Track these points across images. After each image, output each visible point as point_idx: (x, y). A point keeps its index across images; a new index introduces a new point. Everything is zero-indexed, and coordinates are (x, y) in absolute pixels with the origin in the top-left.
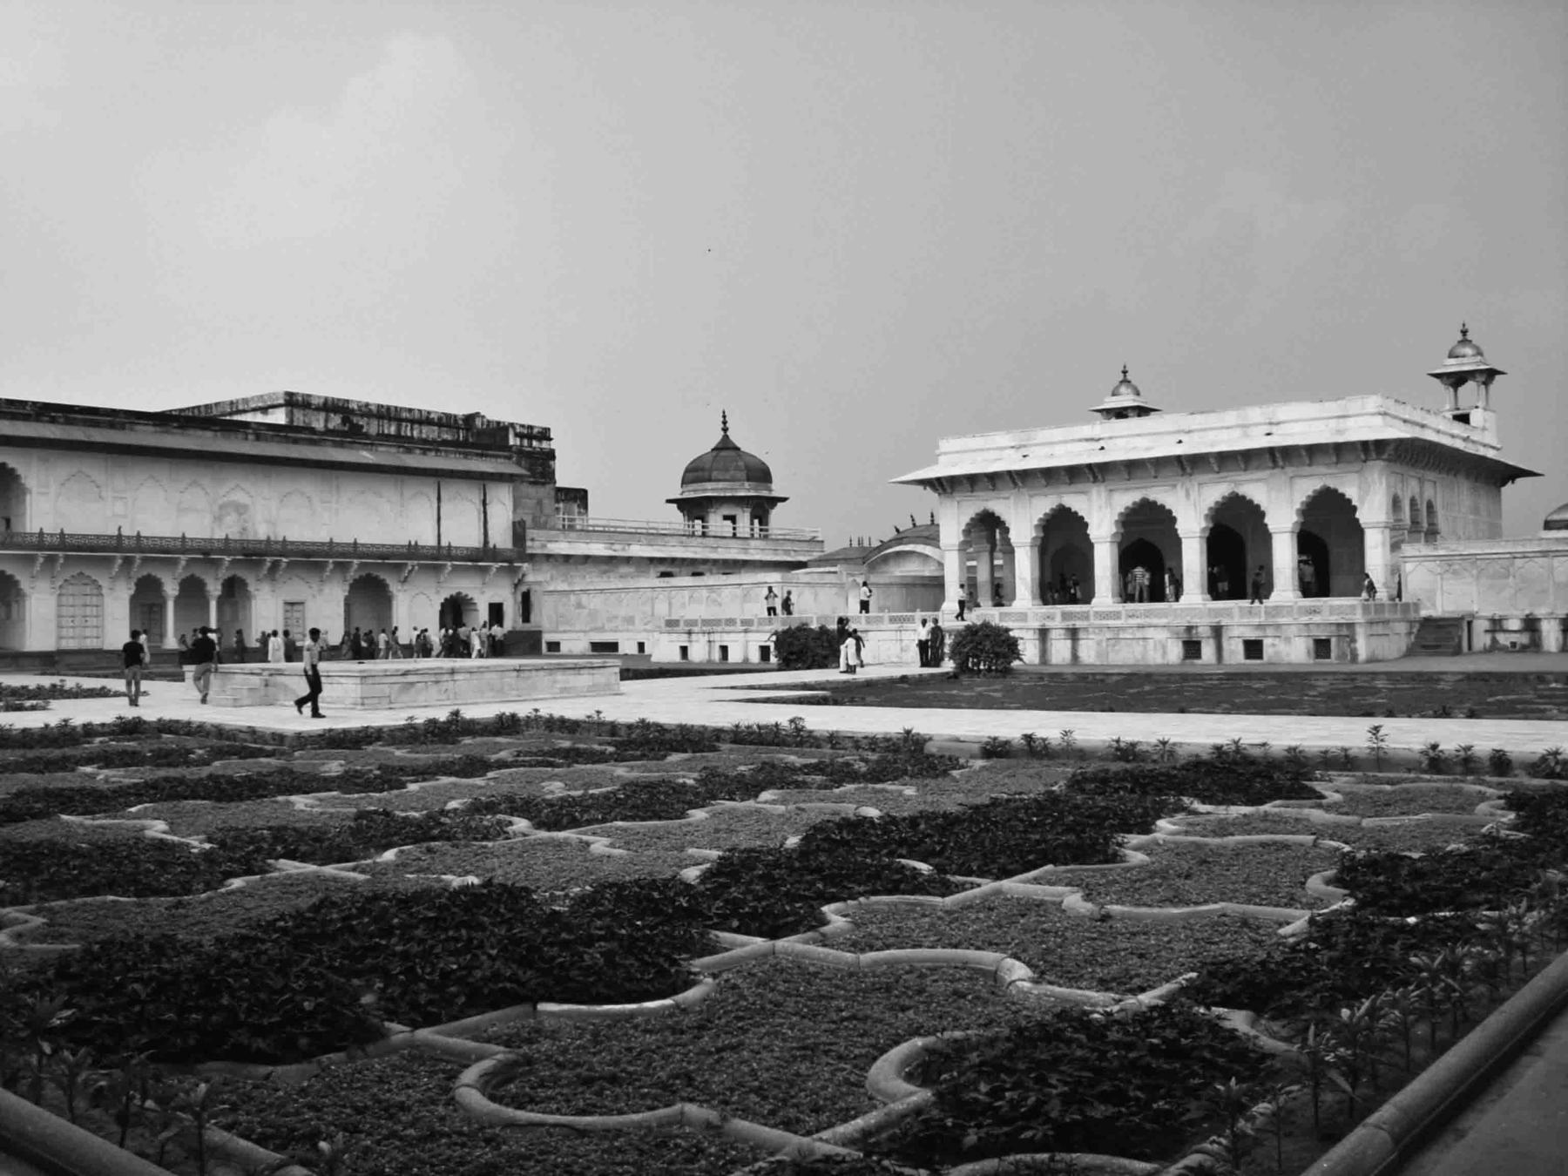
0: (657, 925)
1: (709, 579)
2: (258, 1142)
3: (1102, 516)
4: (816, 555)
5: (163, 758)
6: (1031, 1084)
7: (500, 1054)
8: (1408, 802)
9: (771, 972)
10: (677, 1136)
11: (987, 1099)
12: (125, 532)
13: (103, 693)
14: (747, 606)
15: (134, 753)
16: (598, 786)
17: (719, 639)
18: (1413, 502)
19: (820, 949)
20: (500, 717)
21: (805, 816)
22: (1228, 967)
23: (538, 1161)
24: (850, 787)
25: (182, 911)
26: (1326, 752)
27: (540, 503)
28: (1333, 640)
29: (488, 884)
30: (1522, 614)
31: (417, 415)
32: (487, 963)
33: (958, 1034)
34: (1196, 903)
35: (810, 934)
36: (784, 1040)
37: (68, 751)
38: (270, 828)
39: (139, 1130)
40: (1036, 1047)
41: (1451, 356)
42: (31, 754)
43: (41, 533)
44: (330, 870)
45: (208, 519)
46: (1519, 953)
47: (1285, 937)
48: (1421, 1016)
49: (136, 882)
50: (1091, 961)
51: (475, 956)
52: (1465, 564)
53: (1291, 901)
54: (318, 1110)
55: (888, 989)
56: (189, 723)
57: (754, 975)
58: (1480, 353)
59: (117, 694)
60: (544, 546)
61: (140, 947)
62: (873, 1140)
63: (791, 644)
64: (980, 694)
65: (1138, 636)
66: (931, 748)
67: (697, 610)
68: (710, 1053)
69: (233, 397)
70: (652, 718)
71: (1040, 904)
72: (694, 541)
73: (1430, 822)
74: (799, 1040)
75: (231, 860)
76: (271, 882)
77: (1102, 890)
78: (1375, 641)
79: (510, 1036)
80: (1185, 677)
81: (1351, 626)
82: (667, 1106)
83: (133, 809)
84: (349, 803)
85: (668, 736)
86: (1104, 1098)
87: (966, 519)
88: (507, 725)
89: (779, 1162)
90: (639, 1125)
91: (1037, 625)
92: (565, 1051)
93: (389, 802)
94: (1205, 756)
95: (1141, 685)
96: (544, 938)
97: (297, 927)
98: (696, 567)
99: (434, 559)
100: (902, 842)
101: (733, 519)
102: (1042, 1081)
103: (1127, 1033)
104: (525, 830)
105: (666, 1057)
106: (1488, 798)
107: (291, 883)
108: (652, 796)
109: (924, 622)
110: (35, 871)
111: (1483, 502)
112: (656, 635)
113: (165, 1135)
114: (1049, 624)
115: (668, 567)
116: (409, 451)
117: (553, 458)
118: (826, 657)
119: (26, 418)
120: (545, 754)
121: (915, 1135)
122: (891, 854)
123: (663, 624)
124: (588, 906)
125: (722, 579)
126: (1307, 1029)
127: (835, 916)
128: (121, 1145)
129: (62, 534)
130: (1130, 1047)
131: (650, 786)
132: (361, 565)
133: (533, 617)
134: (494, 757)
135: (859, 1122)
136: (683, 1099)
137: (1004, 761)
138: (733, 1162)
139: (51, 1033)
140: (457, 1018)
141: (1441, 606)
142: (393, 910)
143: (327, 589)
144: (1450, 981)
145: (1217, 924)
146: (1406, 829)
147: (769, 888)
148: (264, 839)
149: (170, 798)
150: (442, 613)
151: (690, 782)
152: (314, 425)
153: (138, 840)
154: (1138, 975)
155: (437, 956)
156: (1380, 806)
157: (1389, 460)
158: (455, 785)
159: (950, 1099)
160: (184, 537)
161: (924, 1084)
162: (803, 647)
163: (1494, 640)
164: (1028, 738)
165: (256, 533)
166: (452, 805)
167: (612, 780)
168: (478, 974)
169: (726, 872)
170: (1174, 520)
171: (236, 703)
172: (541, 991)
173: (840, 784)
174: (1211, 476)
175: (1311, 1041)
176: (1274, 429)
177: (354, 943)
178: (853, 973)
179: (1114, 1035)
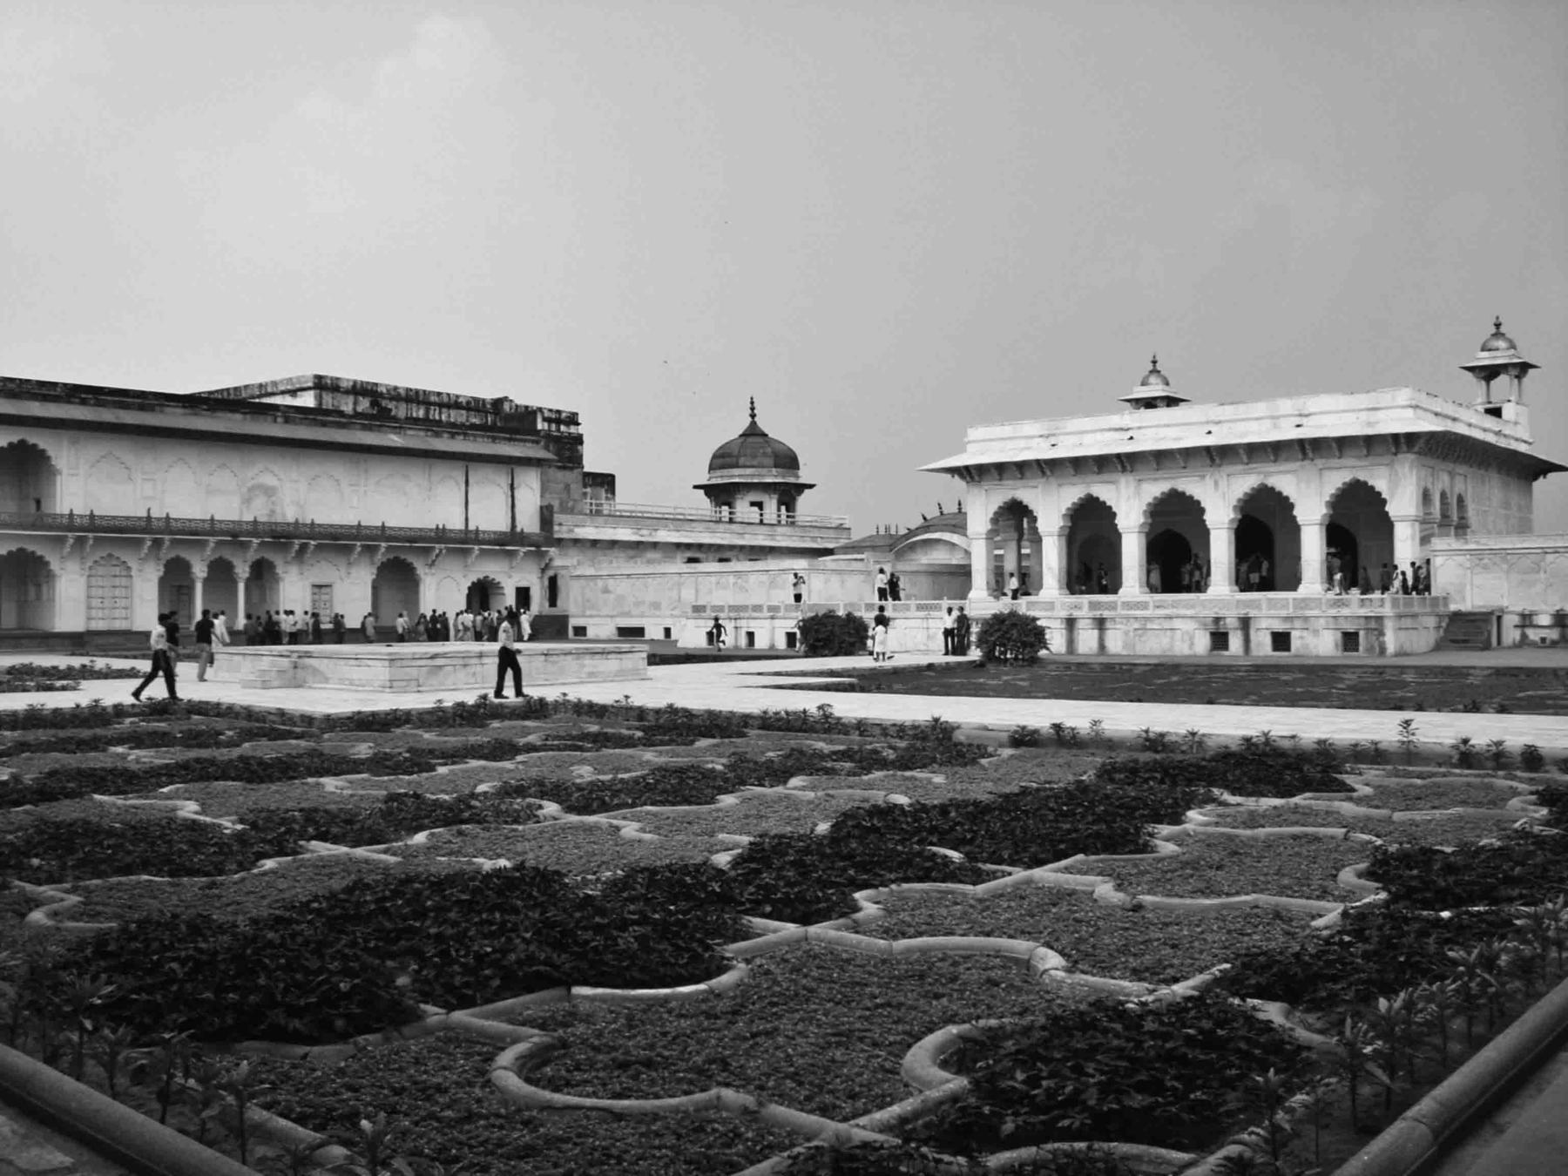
1: (734, 566)
2: (294, 1121)
4: (843, 542)
5: (194, 739)
6: (1068, 1073)
7: (536, 1037)
8: (1439, 796)
9: (807, 958)
10: (715, 1121)
11: (1024, 1087)
12: (154, 514)
14: (773, 592)
15: (165, 734)
16: (628, 770)
17: (746, 625)
18: (1443, 495)
19: (853, 936)
22: (1262, 959)
23: (576, 1144)
26: (1356, 745)
27: (567, 487)
28: (1362, 633)
29: (520, 867)
30: (1553, 610)
31: (446, 399)
32: (522, 946)
33: (993, 1022)
34: (1228, 895)
35: (841, 921)
36: (819, 1026)
37: (99, 731)
38: (301, 810)
39: (178, 1108)
41: (1483, 350)
42: (62, 734)
43: (71, 515)
44: (361, 852)
45: (235, 502)
46: (1554, 948)
47: (1317, 929)
48: (1459, 1011)
49: (169, 862)
50: (1124, 950)
51: (510, 940)
52: (1497, 559)
53: (1324, 894)
54: (355, 1090)
55: (922, 976)
56: (218, 704)
57: (787, 961)
58: (1513, 346)
63: (817, 631)
65: (1170, 627)
66: (959, 736)
70: (681, 703)
71: (1072, 893)
72: (721, 527)
73: (1461, 817)
74: (834, 1026)
75: (264, 841)
76: (303, 864)
77: (1133, 879)
78: (1402, 633)
79: (545, 1020)
80: (1212, 668)
81: (1380, 619)
82: (703, 1090)
83: (165, 790)
84: (379, 786)
85: (696, 721)
86: (1141, 1088)
89: (817, 1148)
91: (1064, 614)
92: (600, 1035)
93: (419, 784)
94: (1234, 748)
96: (578, 921)
98: (722, 553)
99: (461, 543)
100: (933, 830)
101: (760, 505)
102: (1079, 1070)
105: (701, 1042)
106: (1520, 794)
107: (324, 865)
108: (682, 780)
109: (950, 611)
110: (71, 850)
111: (1515, 498)
112: (684, 621)
113: (204, 1114)
114: (1076, 614)
115: (695, 553)
116: (437, 435)
117: (581, 443)
118: (852, 645)
119: (56, 399)
120: (573, 738)
121: (952, 1123)
123: (689, 610)
124: (622, 891)
125: (746, 565)
126: (1342, 1022)
127: (867, 903)
128: (162, 1121)
129: (92, 516)
130: (1166, 1037)
131: (680, 771)
132: (389, 548)
133: (559, 603)
134: (522, 741)
135: (896, 1109)
136: (719, 1084)
138: (770, 1147)
139: (92, 1011)
140: (493, 1001)
141: (1469, 602)
142: (427, 893)
143: (354, 571)
144: (1487, 976)
145: (1248, 915)
146: (1437, 823)
147: (800, 874)
148: (294, 820)
149: (201, 779)
150: (469, 597)
151: (719, 767)
152: (344, 408)
153: (171, 820)
154: (1172, 966)
155: (471, 939)
156: (1411, 799)
157: (1419, 453)
158: (484, 768)
159: (987, 1087)
160: (212, 519)
161: (958, 1072)
162: (829, 634)
163: (1524, 636)
164: (1057, 727)
165: (284, 515)
166: (481, 788)
167: (642, 764)
168: (513, 957)
169: (757, 857)
170: (1202, 511)
171: (265, 685)
174: (1240, 467)
175: (1348, 1033)
176: (1304, 421)
177: (388, 925)
178: (886, 960)
179: (1150, 1025)
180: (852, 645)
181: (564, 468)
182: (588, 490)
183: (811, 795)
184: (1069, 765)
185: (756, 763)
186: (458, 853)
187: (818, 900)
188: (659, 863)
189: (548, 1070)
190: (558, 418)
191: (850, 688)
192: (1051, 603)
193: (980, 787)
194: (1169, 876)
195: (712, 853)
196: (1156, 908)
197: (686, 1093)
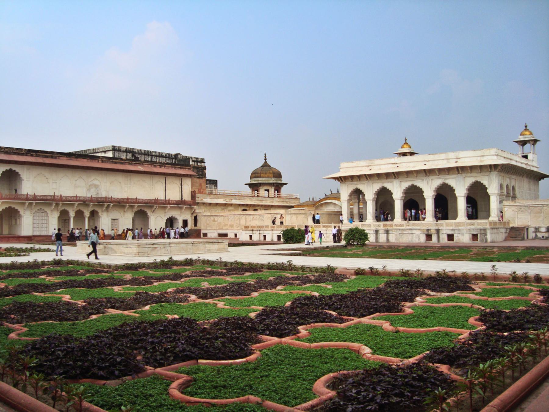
0: (241, 332)
1: (259, 212)
2: (101, 407)
3: (397, 191)
4: (297, 203)
5: (69, 273)
6: (370, 390)
7: (185, 378)
8: (504, 292)
9: (280, 350)
10: (247, 407)
13: (48, 250)
15: (59, 271)
17: (263, 233)
18: (507, 186)
19: (297, 342)
20: (186, 260)
21: (292, 295)
22: (440, 350)
24: (308, 285)
25: (75, 327)
26: (476, 274)
27: (201, 185)
28: (479, 235)
29: (181, 318)
30: (546, 226)
31: (158, 154)
32: (181, 346)
33: (345, 372)
34: (430, 327)
35: (294, 336)
36: (284, 373)
37: (36, 270)
38: (106, 298)
39: (60, 402)
40: (372, 377)
42: (23, 271)
43: (27, 195)
44: (126, 313)
45: (85, 189)
48: (509, 368)
50: (392, 347)
51: (177, 343)
52: (526, 208)
53: (463, 327)
55: (321, 356)
56: (78, 261)
58: (531, 134)
59: (53, 251)
60: (202, 200)
61: (61, 339)
62: (315, 409)
64: (354, 252)
65: (411, 233)
66: (337, 271)
67: (256, 222)
68: (259, 378)
69: (94, 148)
70: (239, 260)
71: (375, 327)
72: (254, 198)
73: (512, 299)
74: (290, 373)
75: (92, 309)
78: (493, 235)
79: (189, 371)
80: (426, 247)
81: (485, 230)
83: (58, 291)
85: (245, 266)
86: (396, 395)
87: (350, 191)
88: (189, 263)
90: (233, 403)
91: (374, 228)
92: (207, 377)
94: (433, 275)
95: (411, 250)
96: (201, 337)
97: (115, 332)
98: (255, 207)
99: (164, 204)
101: (268, 191)
102: (374, 389)
103: (404, 372)
104: (195, 299)
105: (243, 379)
106: (533, 291)
107: (113, 317)
109: (335, 227)
110: (25, 312)
111: (533, 187)
113: (69, 404)
114: (379, 228)
115: (245, 207)
116: (155, 166)
117: (205, 169)
118: (300, 239)
119: (22, 154)
121: (329, 407)
122: (322, 309)
123: (243, 227)
125: (263, 212)
126: (468, 372)
127: (303, 330)
128: (54, 407)
129: (35, 195)
130: (405, 377)
131: (239, 284)
132: (138, 206)
133: (198, 225)
134: (184, 274)
135: (310, 403)
136: (249, 394)
137: (362, 277)
139: (30, 369)
140: (170, 365)
141: (517, 223)
142: (148, 327)
144: (519, 356)
146: (504, 302)
147: (280, 320)
148: (103, 302)
150: (166, 223)
151: (252, 283)
153: (60, 301)
155: (163, 343)
156: (495, 293)
157: (499, 171)
158: (170, 283)
159: (343, 395)
160: (76, 196)
162: (292, 236)
164: (371, 268)
166: (169, 290)
168: (178, 349)
169: (265, 314)
170: (423, 192)
172: (200, 356)
173: (304, 283)
175: (469, 376)
176: (458, 160)
177: (135, 338)
179: (400, 373)
180: (300, 239)
181: (199, 178)
182: (208, 185)
183: (284, 292)
184: (375, 281)
185: (265, 281)
186: (160, 313)
187: (286, 329)
188: (230, 316)
189: (189, 389)
190: (197, 161)
191: (299, 255)
192: (370, 224)
193: (344, 289)
194: (409, 320)
195: (249, 313)
196: (404, 331)
197: (237, 397)
